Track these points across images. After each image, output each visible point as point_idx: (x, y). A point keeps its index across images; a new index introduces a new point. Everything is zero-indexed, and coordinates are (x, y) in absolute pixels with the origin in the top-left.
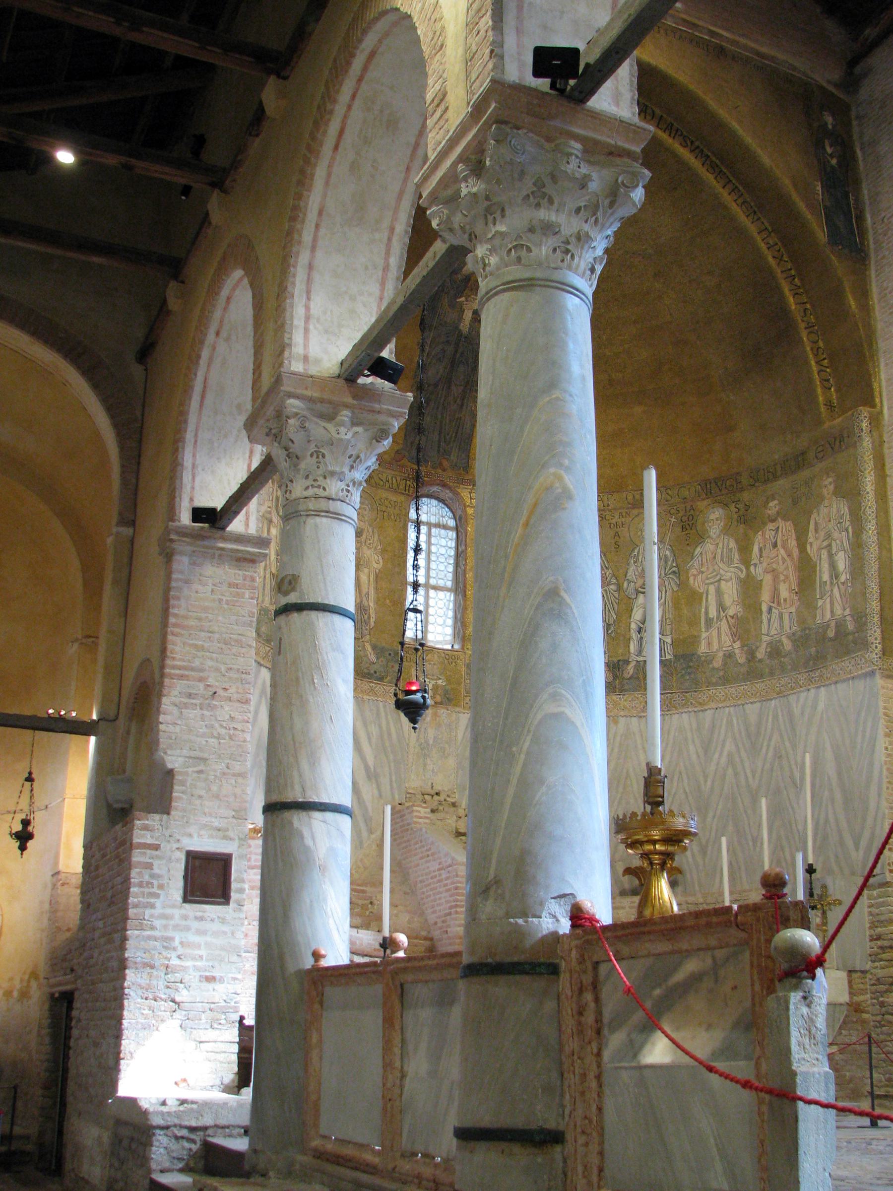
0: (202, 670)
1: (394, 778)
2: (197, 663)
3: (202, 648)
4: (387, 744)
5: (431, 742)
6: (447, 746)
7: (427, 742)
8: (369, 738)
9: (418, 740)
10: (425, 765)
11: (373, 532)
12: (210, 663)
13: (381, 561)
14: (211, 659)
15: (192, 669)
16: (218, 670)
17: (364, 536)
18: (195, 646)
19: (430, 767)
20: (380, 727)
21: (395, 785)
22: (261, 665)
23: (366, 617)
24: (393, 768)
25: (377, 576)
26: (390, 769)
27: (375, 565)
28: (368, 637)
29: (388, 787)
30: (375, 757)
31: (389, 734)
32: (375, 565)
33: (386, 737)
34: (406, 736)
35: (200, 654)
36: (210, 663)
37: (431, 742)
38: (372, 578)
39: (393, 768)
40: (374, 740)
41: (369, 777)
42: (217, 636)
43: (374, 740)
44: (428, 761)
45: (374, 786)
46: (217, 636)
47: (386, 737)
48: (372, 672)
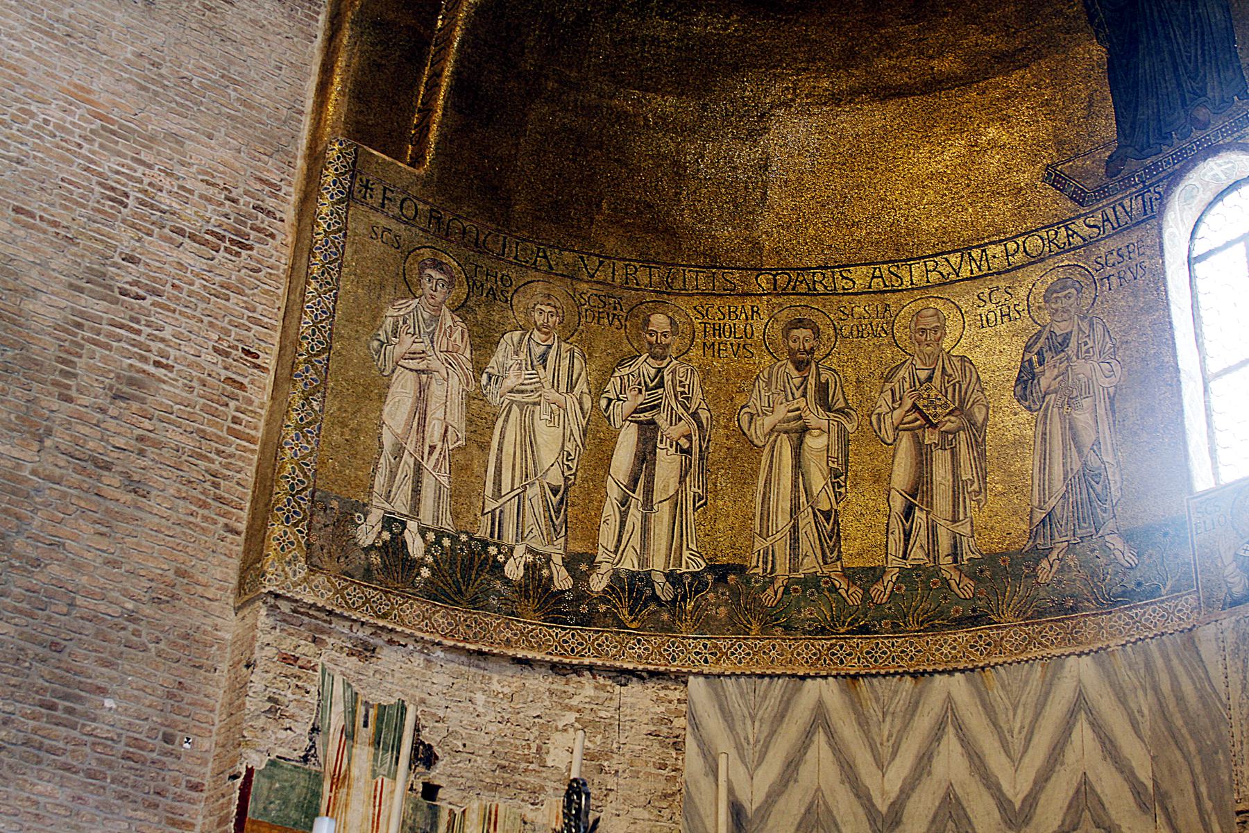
1: (1203, 789)
4: (1179, 722)
8: (1135, 725)
11: (1091, 325)
13: (1117, 368)
17: (1073, 344)
21: (1208, 805)
22: (803, 678)
23: (1098, 488)
24: (1198, 769)
25: (1112, 400)
26: (1192, 772)
27: (1106, 383)
28: (1111, 524)
29: (1194, 816)
30: (1153, 758)
32: (1106, 383)
34: (1220, 687)
38: (1101, 411)
39: (1198, 769)
41: (1143, 807)
45: (1161, 820)
48: (1131, 586)
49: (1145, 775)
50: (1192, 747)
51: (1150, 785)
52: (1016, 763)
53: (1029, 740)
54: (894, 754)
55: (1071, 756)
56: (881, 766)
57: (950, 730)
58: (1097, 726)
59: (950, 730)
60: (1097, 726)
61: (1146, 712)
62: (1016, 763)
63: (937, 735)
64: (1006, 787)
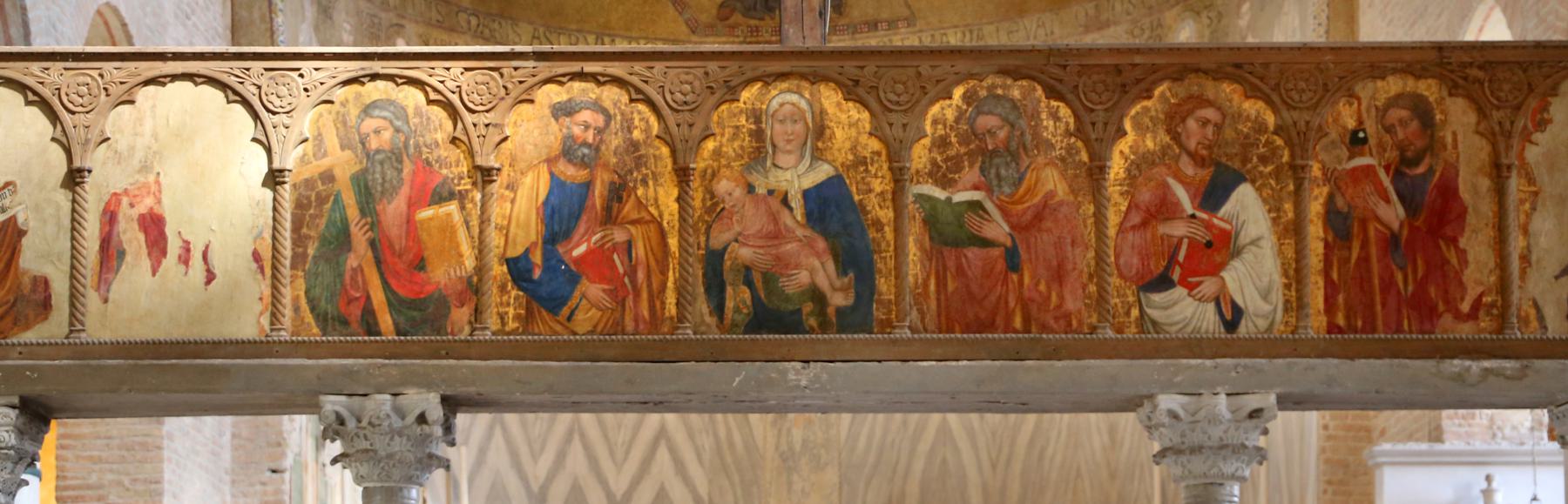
0: (100, 487)
2: (94, 479)
3: (100, 460)
4: (729, 459)
5: (798, 447)
6: (823, 451)
7: (791, 449)
9: (777, 448)
10: (790, 484)
12: (110, 477)
14: (111, 471)
15: (89, 487)
16: (120, 483)
18: (90, 458)
19: (798, 486)
20: (716, 435)
24: (739, 492)
26: (735, 494)
30: (710, 482)
31: (731, 445)
33: (725, 446)
34: (760, 443)
35: (97, 467)
36: (110, 477)
37: (798, 447)
40: (707, 457)
42: (116, 442)
43: (707, 457)
44: (795, 477)
46: (116, 442)
47: (725, 446)
49: (703, 490)
50: (736, 479)
51: (706, 498)
52: (619, 466)
53: (627, 452)
54: (543, 449)
55: (655, 469)
56: (535, 457)
57: (576, 437)
58: (673, 451)
59: (576, 437)
60: (673, 451)
61: (707, 447)
62: (619, 466)
63: (568, 439)
64: (611, 482)
